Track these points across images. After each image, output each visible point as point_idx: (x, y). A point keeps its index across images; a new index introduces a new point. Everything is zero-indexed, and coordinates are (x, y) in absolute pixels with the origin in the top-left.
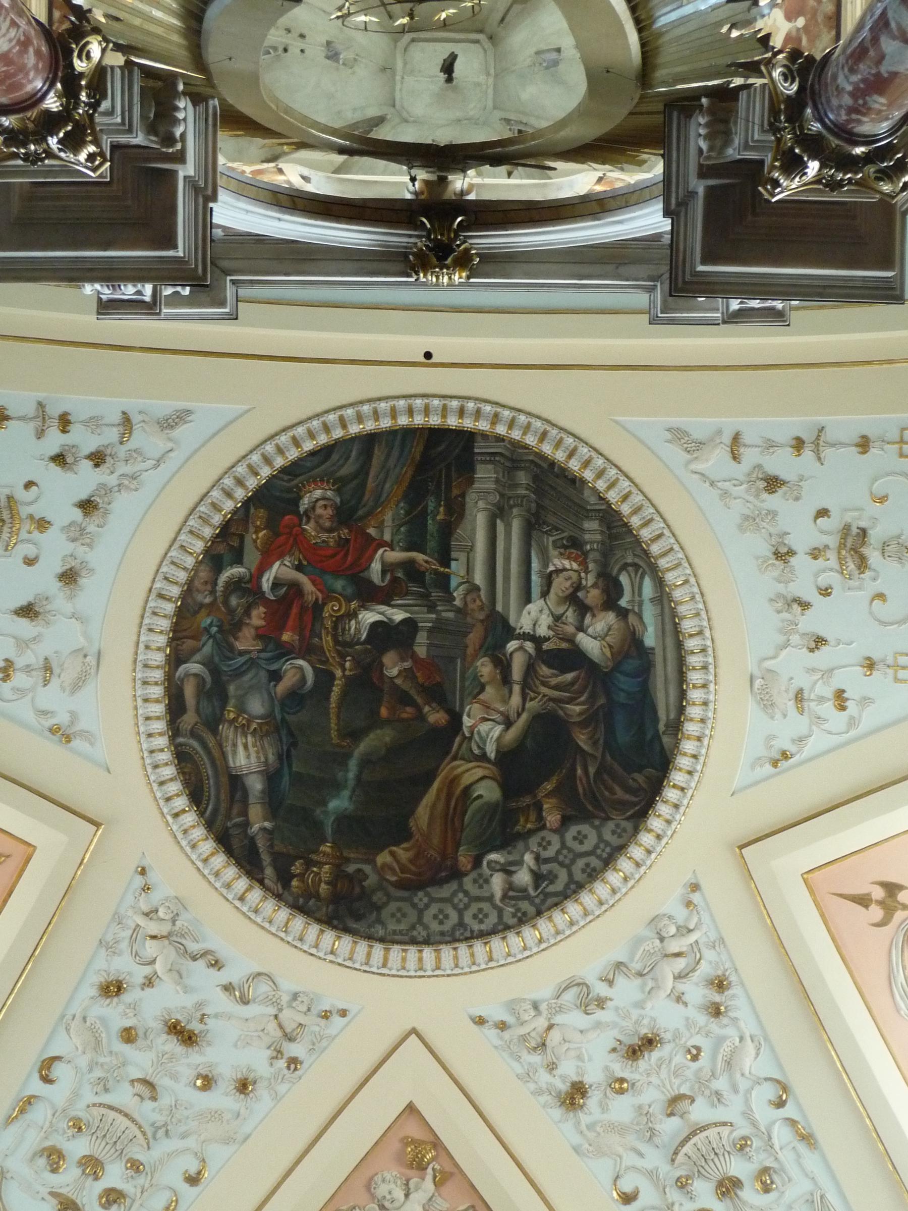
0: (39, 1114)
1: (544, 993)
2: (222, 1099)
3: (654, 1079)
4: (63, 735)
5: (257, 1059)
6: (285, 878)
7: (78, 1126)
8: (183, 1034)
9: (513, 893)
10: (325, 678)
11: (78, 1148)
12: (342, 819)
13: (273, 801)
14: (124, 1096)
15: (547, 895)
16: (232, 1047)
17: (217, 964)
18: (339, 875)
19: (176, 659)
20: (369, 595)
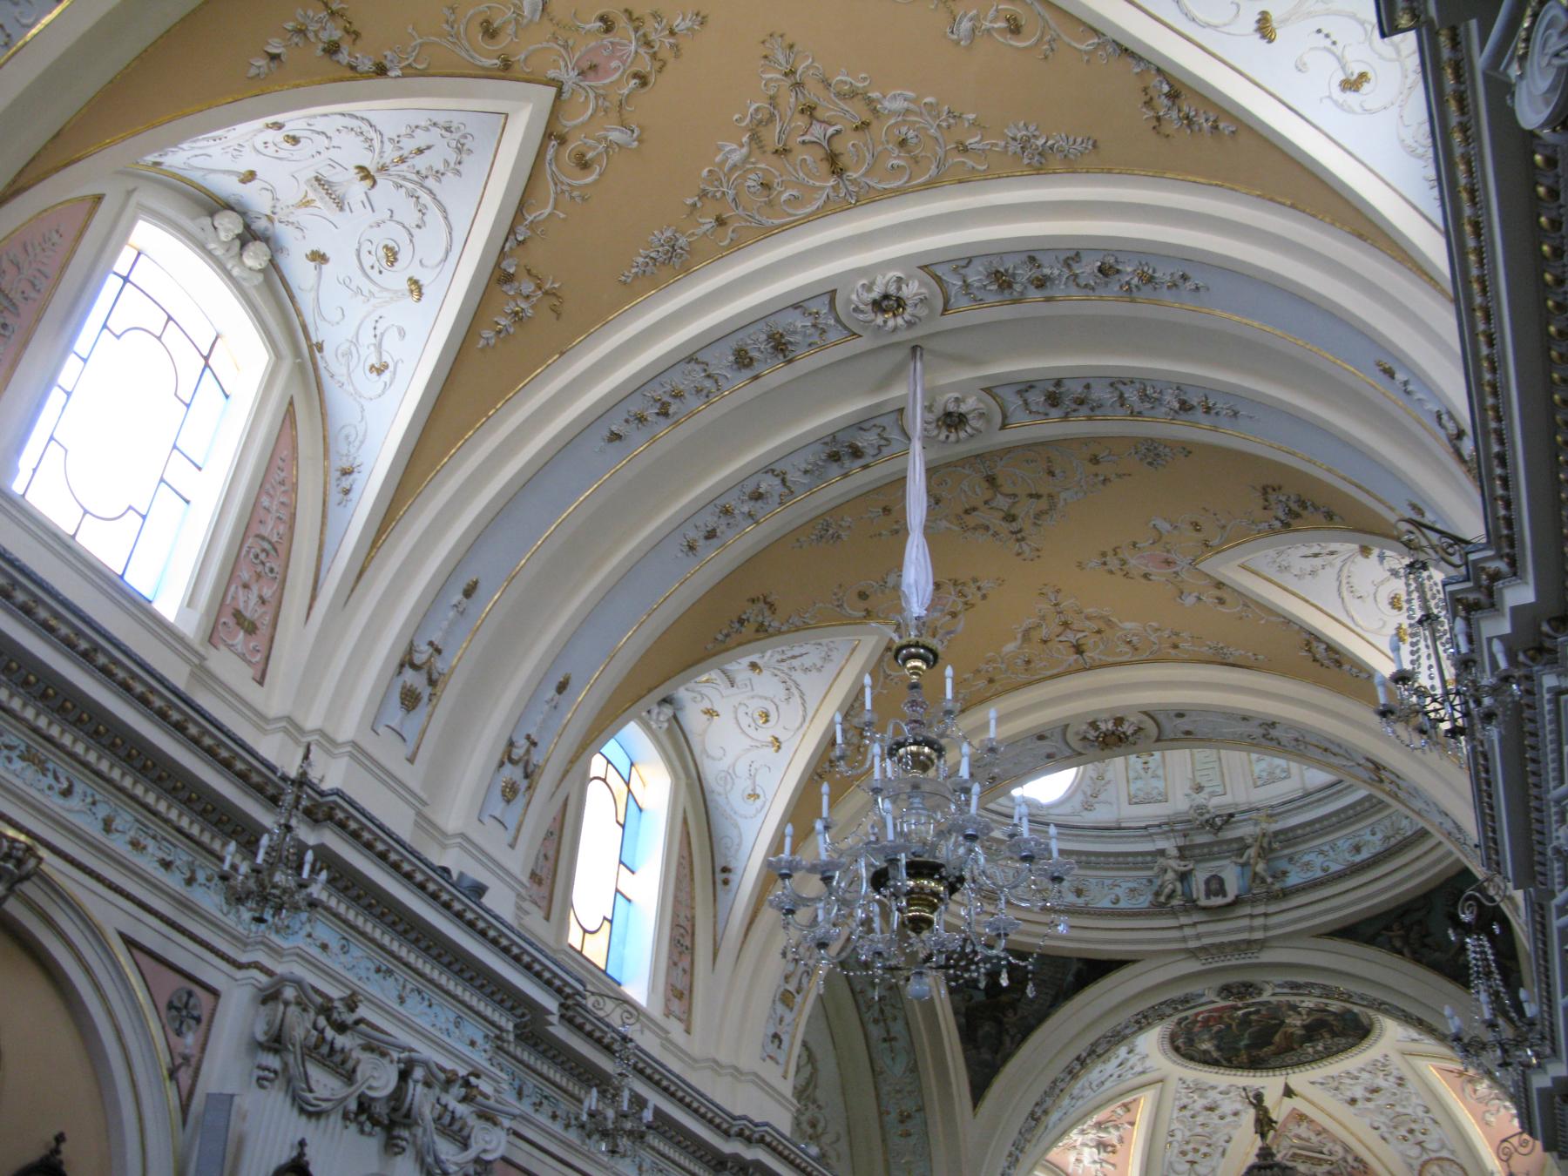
1: (1335, 1073)
2: (1230, 1119)
3: (1380, 1100)
6: (1229, 1061)
7: (1187, 1143)
8: (1211, 1109)
9: (1316, 1052)
11: (1190, 1147)
12: (1248, 1047)
13: (1218, 1048)
14: (1199, 1130)
15: (1329, 1054)
16: (1227, 1106)
17: (1213, 1088)
18: (1249, 1056)
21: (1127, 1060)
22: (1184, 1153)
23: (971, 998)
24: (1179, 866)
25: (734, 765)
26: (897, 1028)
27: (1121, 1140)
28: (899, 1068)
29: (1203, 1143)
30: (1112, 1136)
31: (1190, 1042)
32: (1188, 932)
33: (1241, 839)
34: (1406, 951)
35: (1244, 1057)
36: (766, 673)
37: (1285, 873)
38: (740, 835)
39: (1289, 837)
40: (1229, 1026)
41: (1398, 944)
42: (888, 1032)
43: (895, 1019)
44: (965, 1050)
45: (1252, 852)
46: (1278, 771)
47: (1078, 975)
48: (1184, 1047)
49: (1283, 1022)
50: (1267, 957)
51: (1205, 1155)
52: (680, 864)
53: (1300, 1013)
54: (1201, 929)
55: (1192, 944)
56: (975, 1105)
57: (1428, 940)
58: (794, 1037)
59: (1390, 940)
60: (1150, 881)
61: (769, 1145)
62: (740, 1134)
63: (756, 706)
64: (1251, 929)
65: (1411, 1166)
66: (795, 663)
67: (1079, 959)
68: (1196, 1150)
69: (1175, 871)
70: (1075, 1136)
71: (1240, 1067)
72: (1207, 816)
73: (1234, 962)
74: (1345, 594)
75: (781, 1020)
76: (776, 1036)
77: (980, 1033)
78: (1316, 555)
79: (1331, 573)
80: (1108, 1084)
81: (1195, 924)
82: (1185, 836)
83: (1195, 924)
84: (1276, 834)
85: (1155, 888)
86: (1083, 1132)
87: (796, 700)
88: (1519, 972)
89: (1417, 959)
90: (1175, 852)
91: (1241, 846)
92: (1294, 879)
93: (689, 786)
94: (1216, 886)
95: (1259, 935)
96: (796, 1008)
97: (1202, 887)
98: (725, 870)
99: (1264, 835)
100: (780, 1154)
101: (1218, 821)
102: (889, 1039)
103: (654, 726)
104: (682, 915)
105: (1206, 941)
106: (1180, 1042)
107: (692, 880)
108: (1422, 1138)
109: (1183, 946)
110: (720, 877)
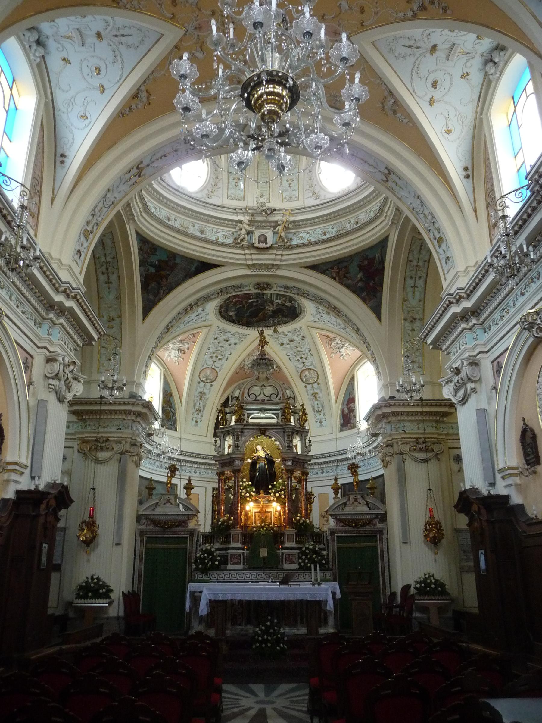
0: (209, 353)
3: (293, 345)
4: (205, 321)
5: (237, 341)
6: (239, 322)
7: (214, 353)
8: (227, 341)
10: (243, 306)
11: (215, 355)
13: (236, 315)
14: (219, 348)
16: (232, 341)
17: (229, 332)
19: (220, 309)
20: (251, 299)
21: (200, 314)
22: (212, 357)
23: (149, 270)
24: (249, 228)
25: (74, 97)
26: (113, 278)
27: (188, 349)
28: (111, 297)
29: (219, 354)
30: (185, 347)
31: (227, 311)
32: (248, 257)
33: (277, 222)
34: (337, 278)
35: (245, 321)
36: (105, 42)
37: (291, 240)
38: (73, 139)
39: (297, 224)
40: (243, 306)
41: (334, 275)
42: (109, 279)
43: (113, 273)
44: (142, 293)
45: (280, 228)
46: (294, 197)
47: (197, 268)
48: (224, 313)
49: (265, 308)
50: (279, 272)
51: (220, 359)
52: (38, 145)
53: (273, 305)
54: (254, 256)
55: (249, 262)
56: (143, 319)
57: (347, 275)
58: (86, 255)
59: (332, 272)
60: (233, 233)
61: (78, 300)
62: (64, 291)
63: (95, 62)
64: (275, 260)
65: (298, 371)
66: (123, 39)
67: (198, 261)
68: (217, 357)
69: (246, 230)
70: (171, 345)
71: (243, 325)
72: (265, 208)
73: (265, 273)
74: (414, 74)
75: (82, 245)
76: (79, 251)
77: (150, 287)
78: (410, 47)
79: (412, 59)
80: (190, 323)
81: (251, 254)
82: (252, 216)
83: (251, 254)
84: (294, 222)
85: (234, 236)
86: (174, 343)
87: (119, 64)
88: (382, 291)
89: (341, 283)
90: (247, 222)
91: (276, 224)
92: (294, 242)
93: (46, 104)
94: (263, 239)
95: (278, 263)
96: (89, 240)
97: (257, 239)
98: (62, 155)
99: (287, 221)
100: (82, 307)
101: (269, 212)
102: (108, 282)
103: (32, 57)
104: (37, 173)
105: (255, 262)
106: (222, 310)
107: (43, 157)
108: (304, 360)
109: (245, 262)
110: (59, 159)
